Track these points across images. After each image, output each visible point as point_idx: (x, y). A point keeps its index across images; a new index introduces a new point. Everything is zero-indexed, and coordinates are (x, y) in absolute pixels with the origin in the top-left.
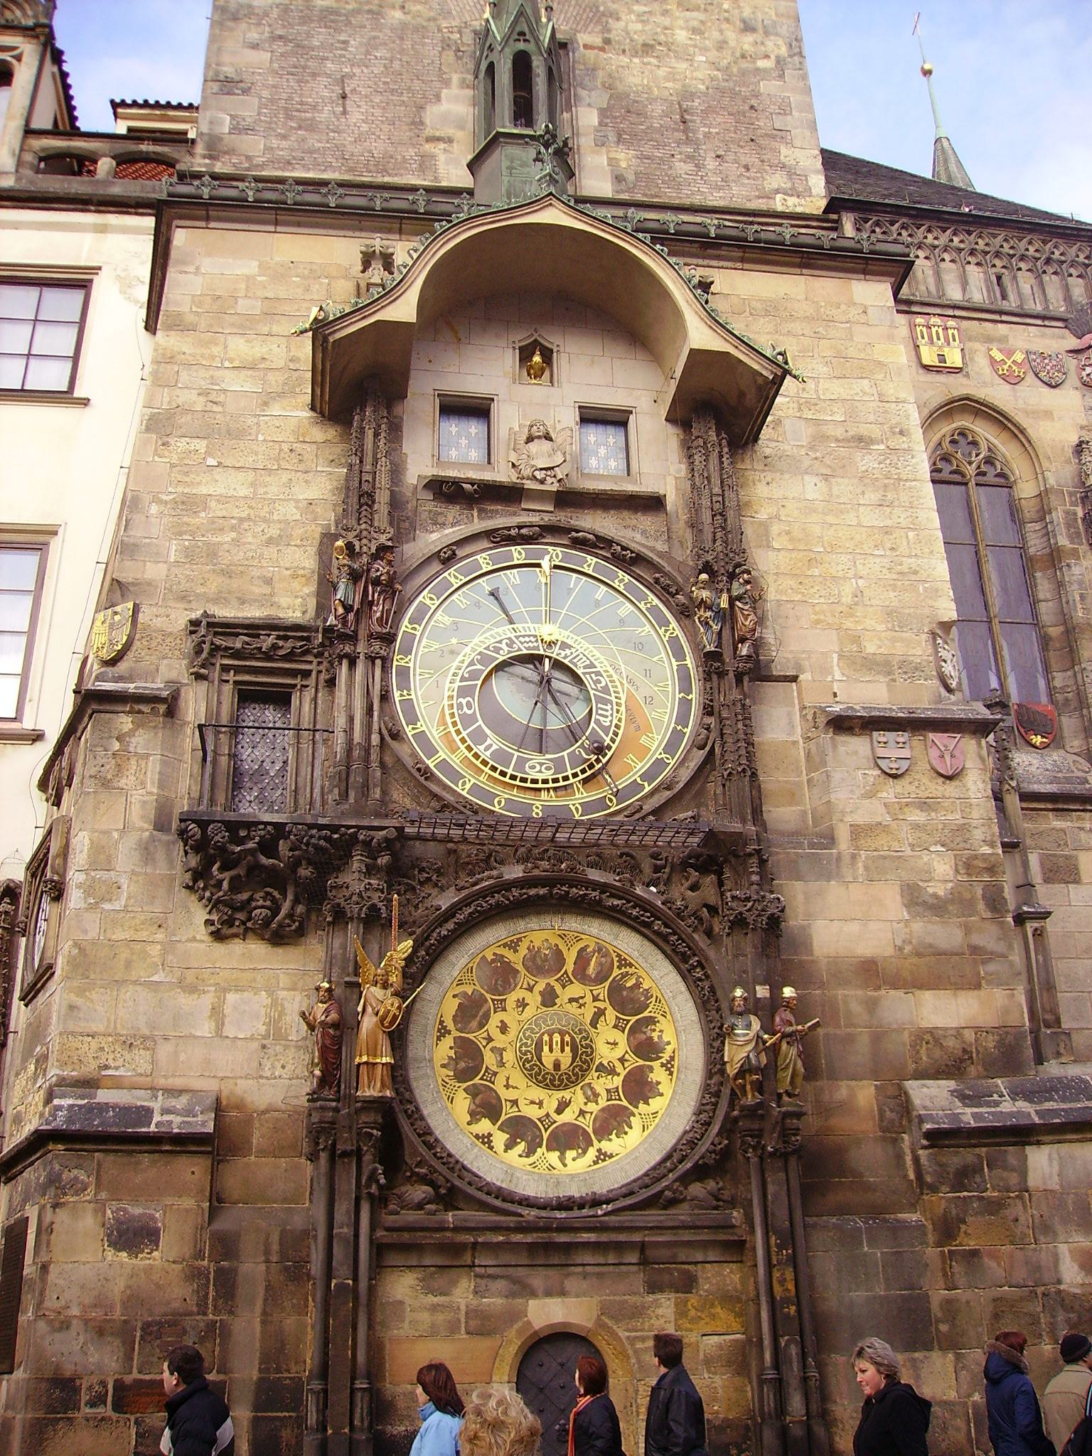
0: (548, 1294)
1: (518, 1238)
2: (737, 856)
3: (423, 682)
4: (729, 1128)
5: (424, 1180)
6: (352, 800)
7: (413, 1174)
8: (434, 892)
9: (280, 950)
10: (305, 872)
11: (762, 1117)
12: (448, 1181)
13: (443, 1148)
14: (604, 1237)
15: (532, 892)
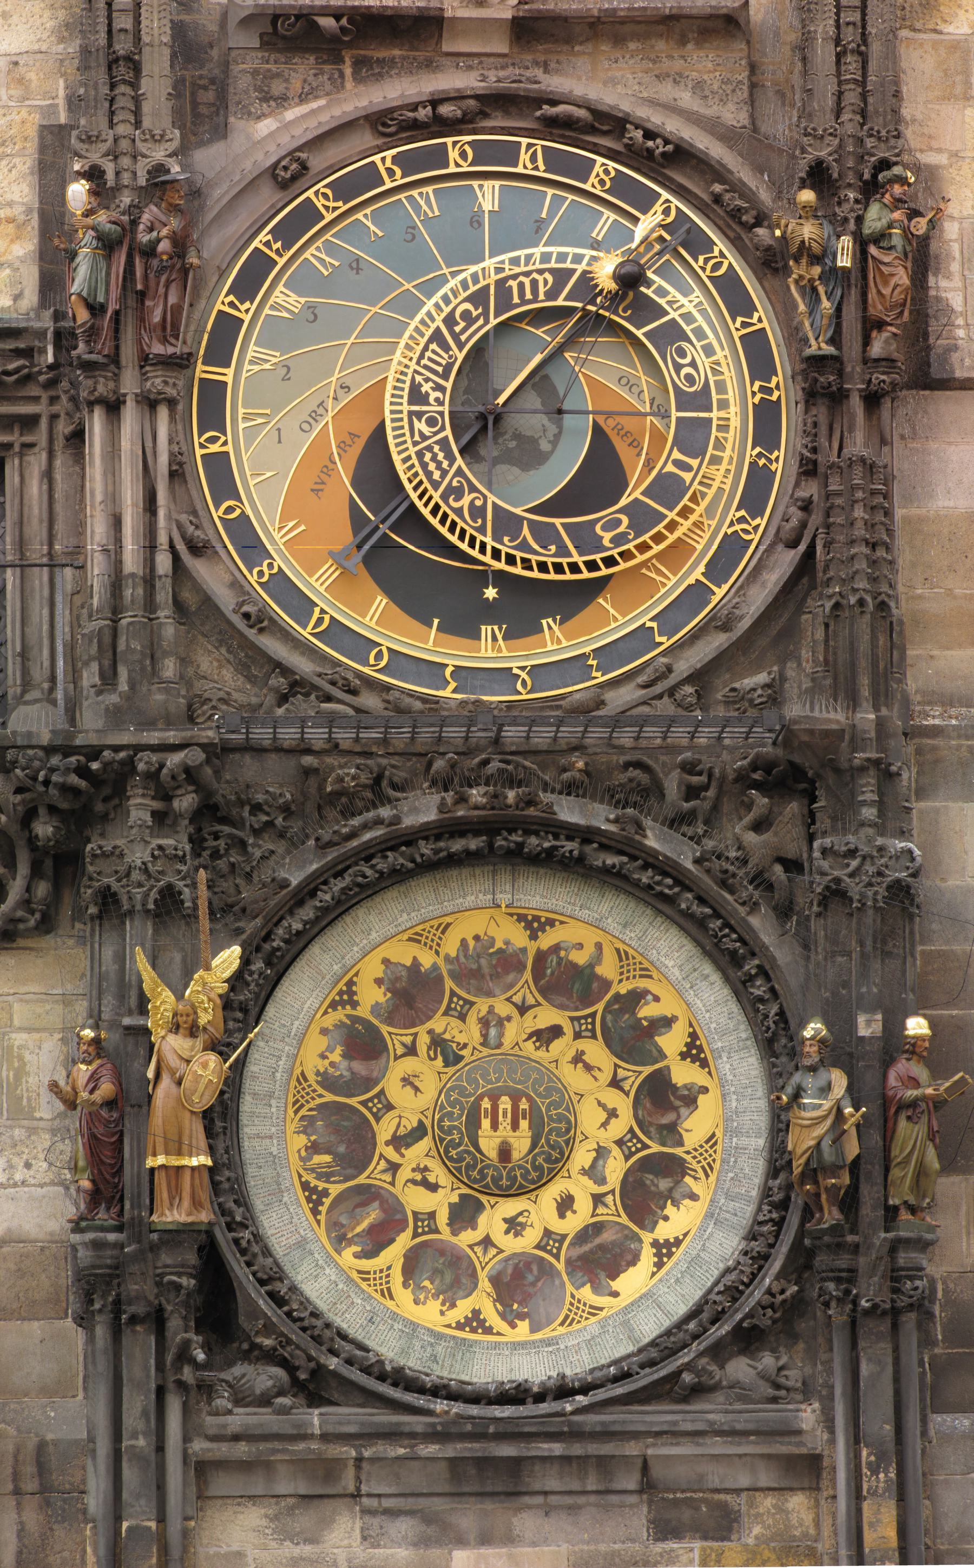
0: (485, 1540)
1: (430, 1450)
2: (837, 771)
3: (252, 433)
4: (801, 1262)
5: (271, 1357)
6: (123, 686)
7: (254, 1346)
8: (280, 847)
9: (12, 962)
10: (44, 829)
11: (855, 1249)
12: (310, 1359)
13: (305, 1302)
14: (577, 1449)
15: (457, 846)
